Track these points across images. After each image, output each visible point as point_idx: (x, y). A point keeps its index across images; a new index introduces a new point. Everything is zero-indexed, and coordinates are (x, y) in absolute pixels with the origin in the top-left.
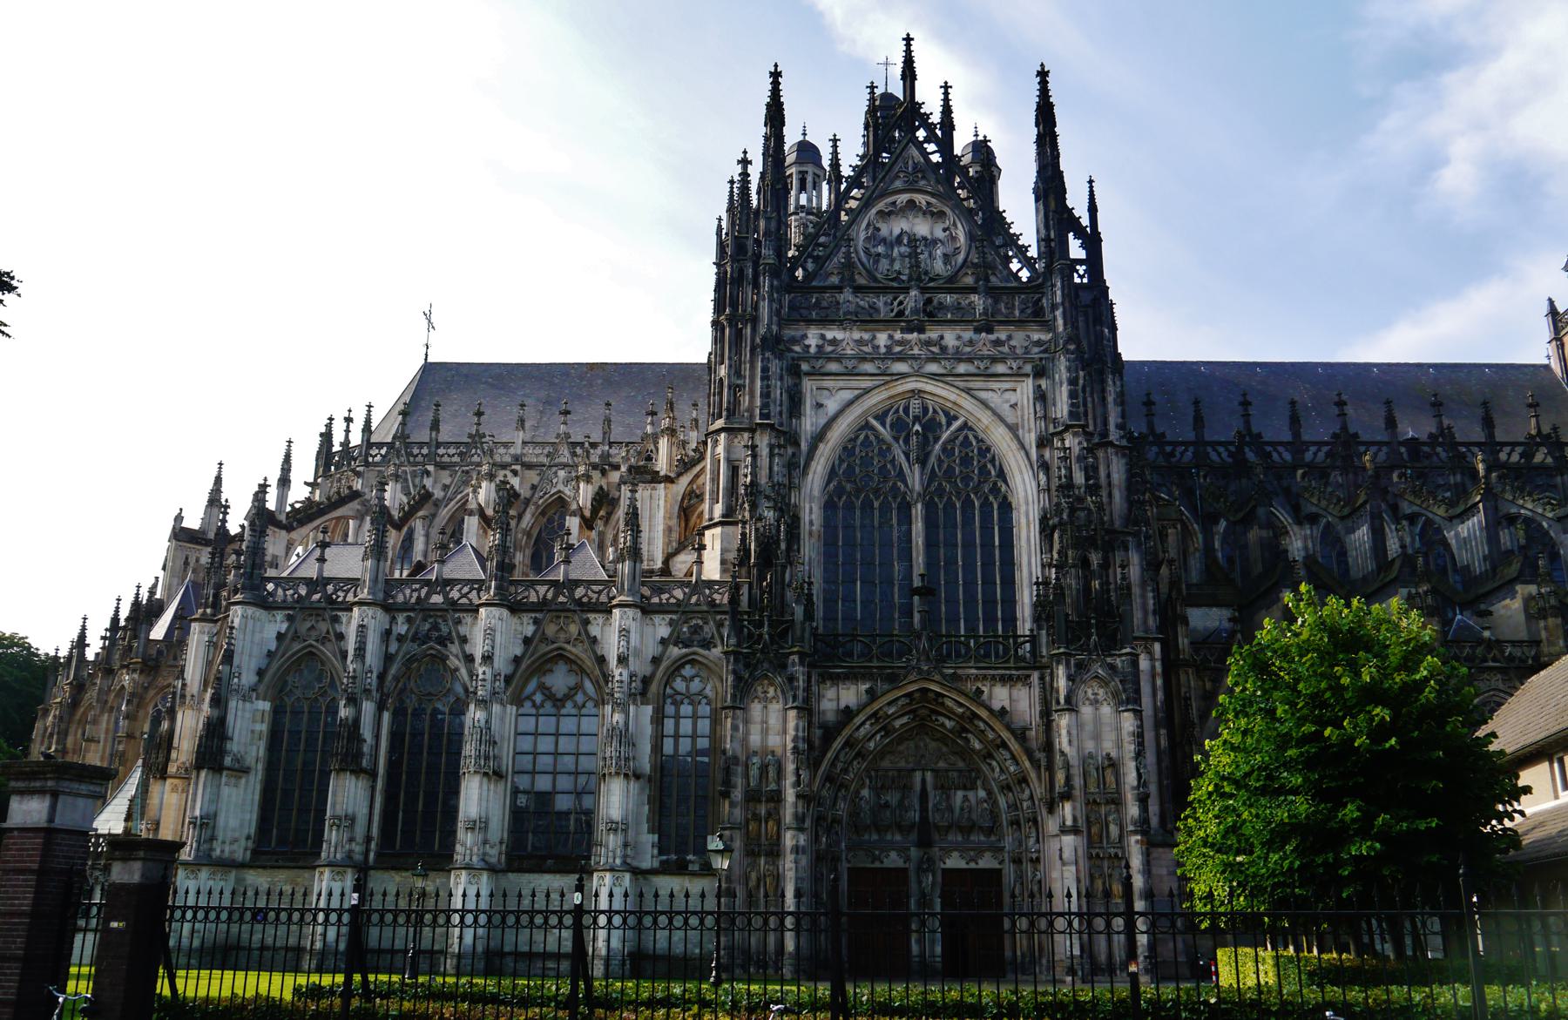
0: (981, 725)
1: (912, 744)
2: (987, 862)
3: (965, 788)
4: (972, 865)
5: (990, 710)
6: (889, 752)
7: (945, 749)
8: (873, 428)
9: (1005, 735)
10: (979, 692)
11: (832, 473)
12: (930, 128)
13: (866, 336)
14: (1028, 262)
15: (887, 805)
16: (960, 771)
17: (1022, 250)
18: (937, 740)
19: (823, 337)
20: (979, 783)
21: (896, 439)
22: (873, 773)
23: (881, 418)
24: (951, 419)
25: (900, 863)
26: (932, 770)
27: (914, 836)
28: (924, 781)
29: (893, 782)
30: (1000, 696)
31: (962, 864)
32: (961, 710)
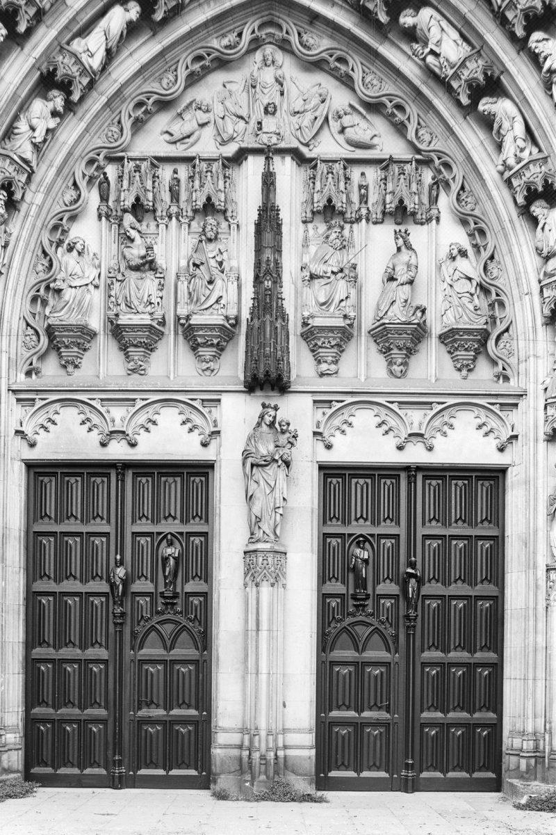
1: (237, 78)
3: (401, 213)
4: (416, 455)
6: (164, 105)
7: (340, 98)
15: (148, 265)
16: (384, 164)
18: (317, 65)
20: (445, 202)
22: (111, 171)
25: (185, 447)
26: (300, 159)
27: (233, 364)
28: (268, 181)
29: (175, 196)
31: (383, 451)
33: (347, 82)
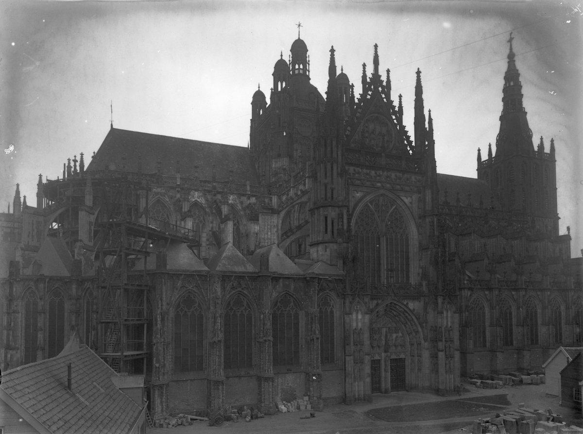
0: (407, 315)
2: (402, 356)
5: (410, 309)
8: (369, 206)
9: (414, 317)
10: (407, 303)
11: (357, 223)
12: (383, 87)
13: (368, 171)
14: (412, 148)
17: (410, 142)
19: (355, 170)
21: (376, 211)
23: (371, 202)
24: (392, 205)
30: (411, 305)
32: (401, 309)
33: (392, 320)
